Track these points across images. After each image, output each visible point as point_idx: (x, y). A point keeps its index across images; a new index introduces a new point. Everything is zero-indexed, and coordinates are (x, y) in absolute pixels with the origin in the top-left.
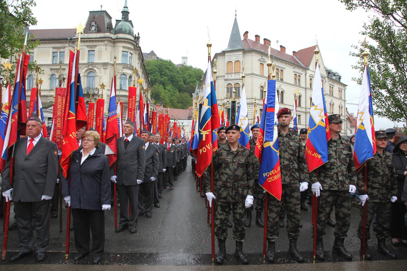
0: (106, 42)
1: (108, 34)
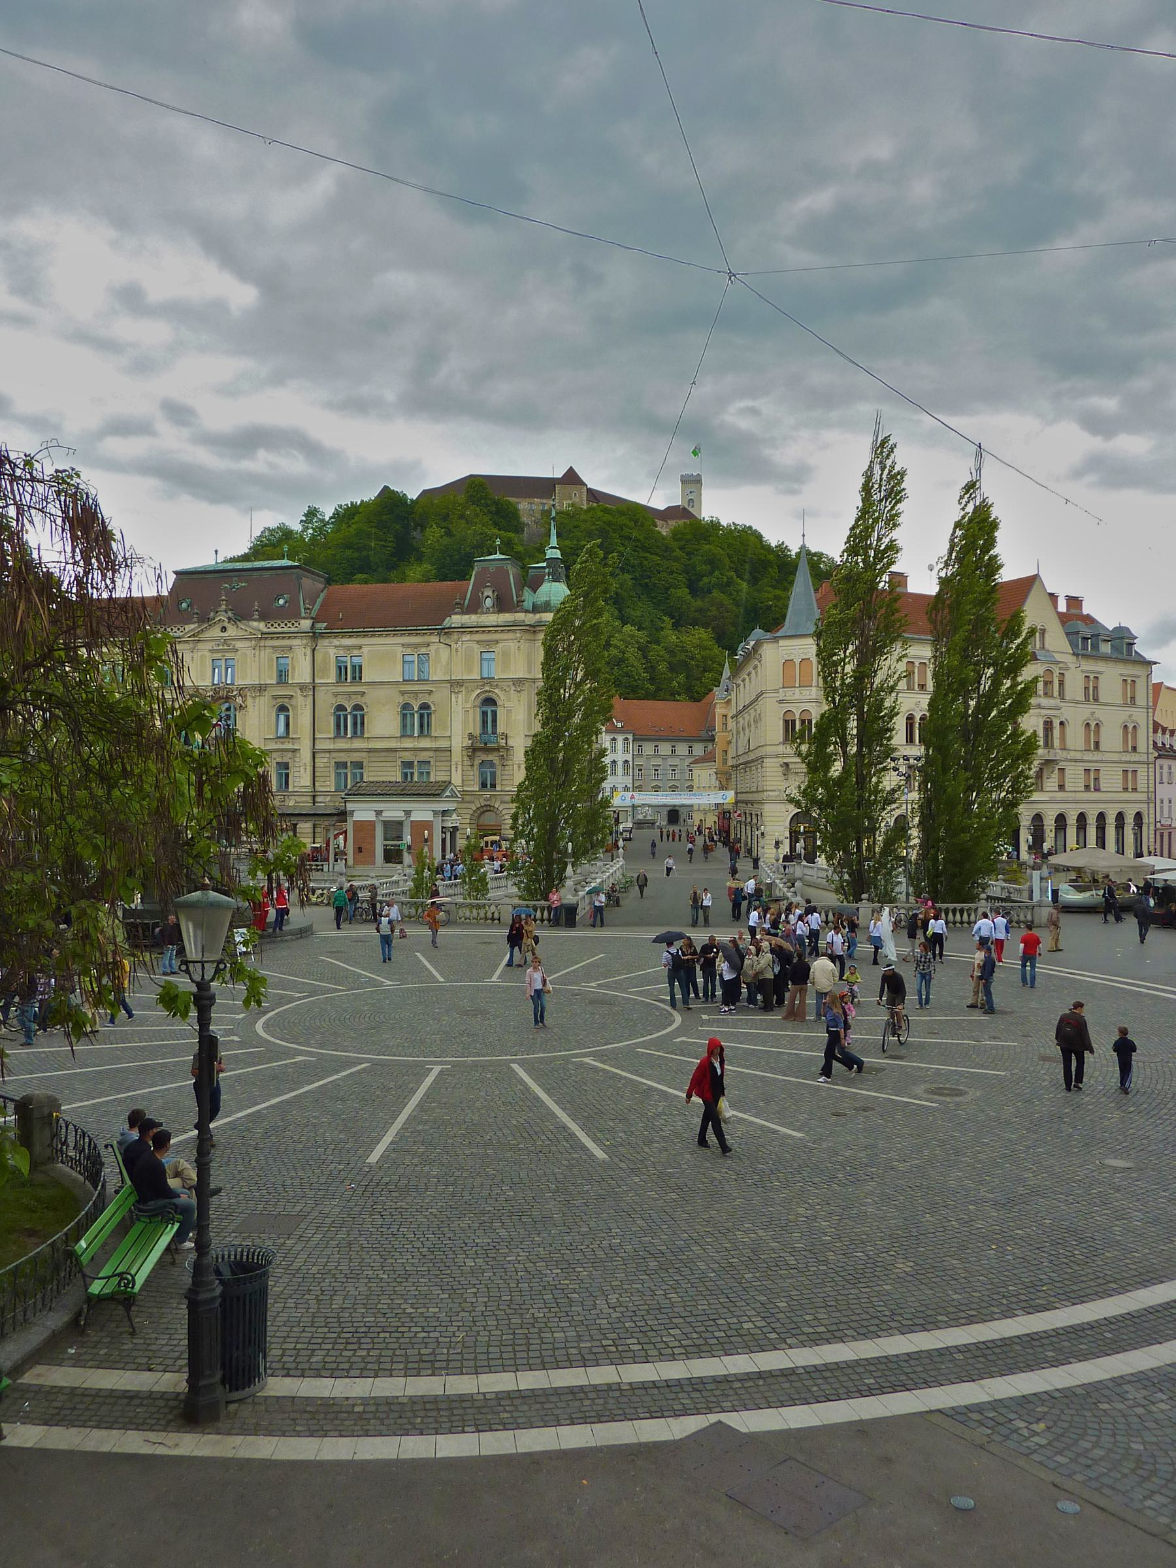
0: (518, 635)
1: (520, 616)
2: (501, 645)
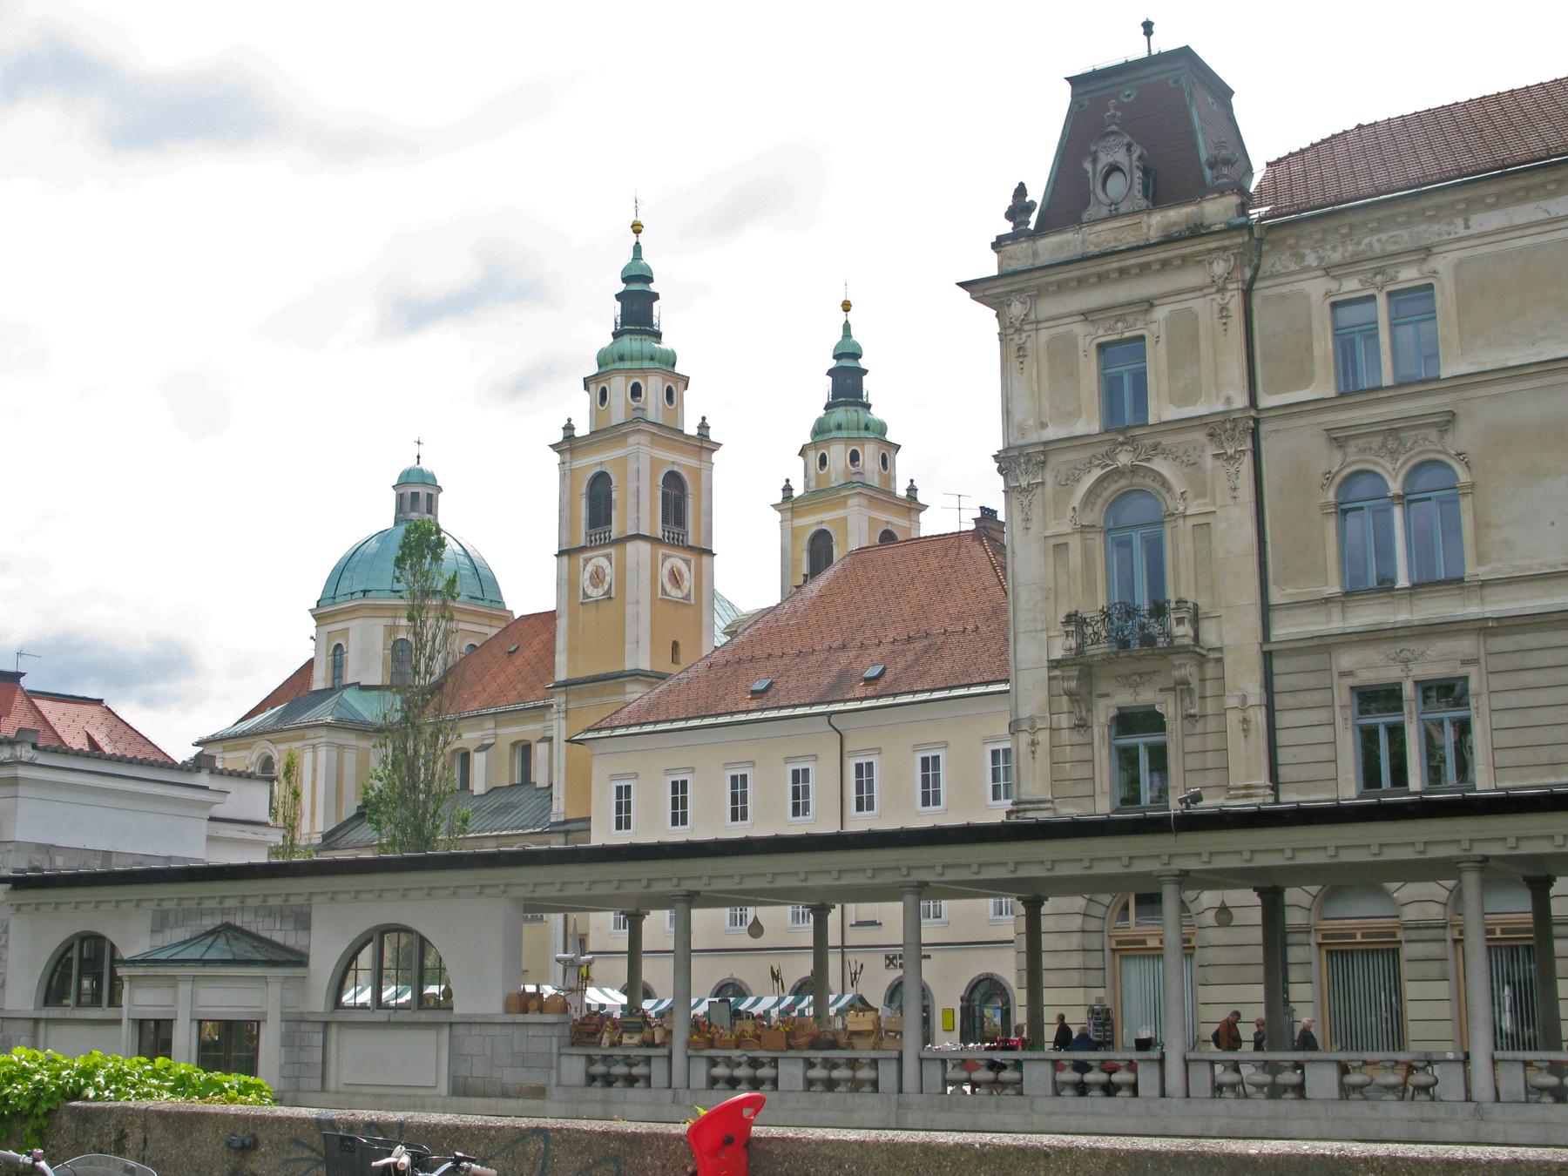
0: (1219, 268)
2: (1160, 313)
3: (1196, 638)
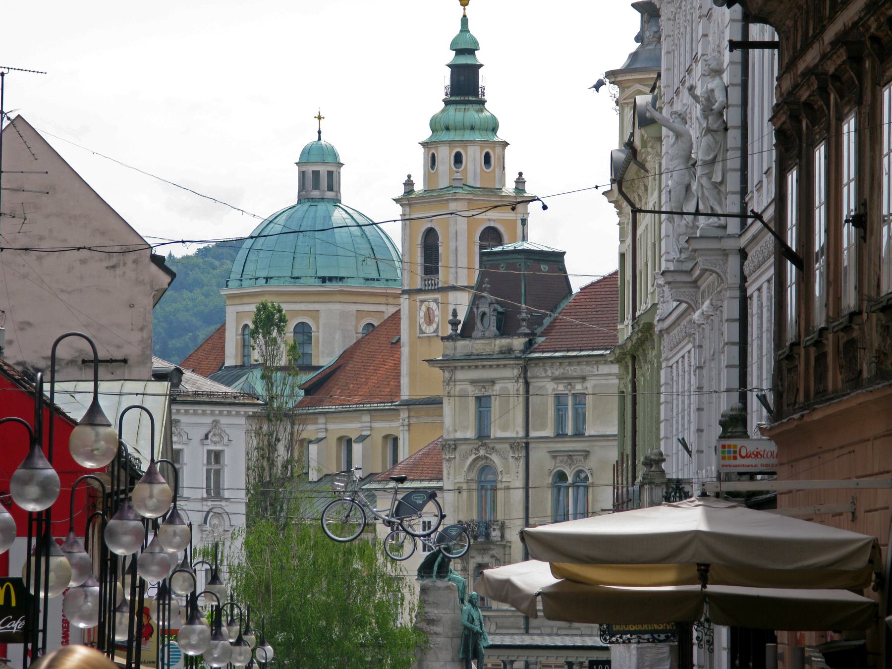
2: (497, 387)
3: (502, 536)
